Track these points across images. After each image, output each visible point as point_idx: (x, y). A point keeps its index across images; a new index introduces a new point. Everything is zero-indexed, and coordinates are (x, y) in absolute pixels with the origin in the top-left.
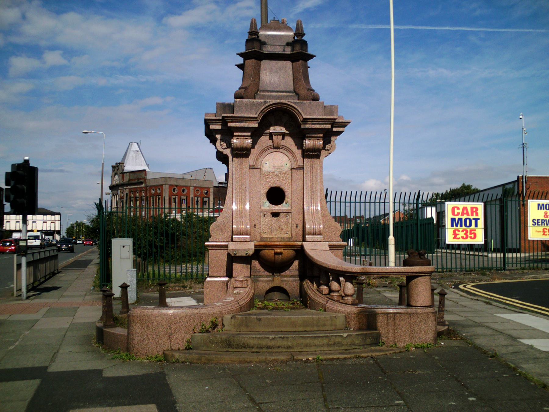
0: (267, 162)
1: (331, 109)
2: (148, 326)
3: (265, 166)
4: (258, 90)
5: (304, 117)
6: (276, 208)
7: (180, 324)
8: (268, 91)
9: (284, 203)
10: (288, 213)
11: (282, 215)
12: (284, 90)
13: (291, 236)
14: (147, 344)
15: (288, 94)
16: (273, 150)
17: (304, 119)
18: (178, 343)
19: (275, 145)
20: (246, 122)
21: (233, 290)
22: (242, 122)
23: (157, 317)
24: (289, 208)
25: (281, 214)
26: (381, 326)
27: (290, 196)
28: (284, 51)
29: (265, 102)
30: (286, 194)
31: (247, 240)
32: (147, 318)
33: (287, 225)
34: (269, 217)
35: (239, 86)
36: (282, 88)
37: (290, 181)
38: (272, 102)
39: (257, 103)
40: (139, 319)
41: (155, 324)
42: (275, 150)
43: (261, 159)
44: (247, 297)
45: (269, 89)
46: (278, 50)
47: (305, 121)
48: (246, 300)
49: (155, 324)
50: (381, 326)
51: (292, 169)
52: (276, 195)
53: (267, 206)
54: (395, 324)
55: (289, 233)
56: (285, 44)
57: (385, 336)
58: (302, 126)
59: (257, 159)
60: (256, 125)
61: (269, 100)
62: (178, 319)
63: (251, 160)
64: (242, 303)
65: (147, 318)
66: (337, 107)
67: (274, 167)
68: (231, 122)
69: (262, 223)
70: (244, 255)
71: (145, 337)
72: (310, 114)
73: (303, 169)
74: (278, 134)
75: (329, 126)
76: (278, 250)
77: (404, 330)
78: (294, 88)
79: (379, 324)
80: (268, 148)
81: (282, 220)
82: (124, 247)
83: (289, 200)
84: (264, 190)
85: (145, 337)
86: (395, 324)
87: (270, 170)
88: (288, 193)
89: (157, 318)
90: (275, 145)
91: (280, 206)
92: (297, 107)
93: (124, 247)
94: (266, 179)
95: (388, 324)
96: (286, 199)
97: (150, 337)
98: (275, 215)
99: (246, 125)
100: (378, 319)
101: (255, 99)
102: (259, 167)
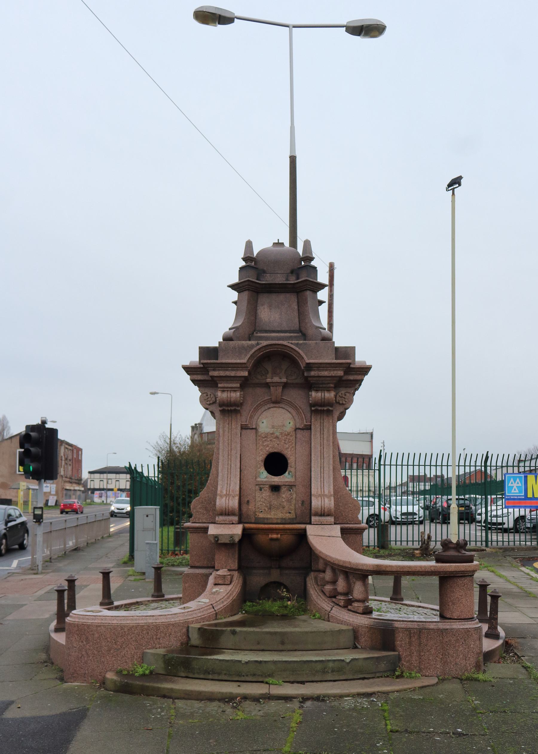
0: (264, 421)
1: (349, 352)
2: (87, 638)
3: (261, 425)
4: (255, 330)
5: (308, 361)
6: (276, 480)
7: (129, 637)
8: (266, 331)
9: (287, 472)
10: (291, 486)
11: (283, 489)
12: (287, 329)
13: (294, 517)
14: (86, 662)
15: (292, 334)
16: (272, 405)
17: (308, 364)
18: (126, 662)
19: (273, 400)
20: (232, 370)
21: (212, 589)
22: (227, 370)
23: (100, 626)
24: (293, 480)
25: (283, 487)
26: (401, 646)
27: (293, 464)
28: (287, 280)
29: (258, 344)
30: (289, 461)
31: (234, 522)
32: (86, 628)
33: (289, 501)
34: (266, 493)
35: (230, 327)
36: (285, 327)
37: (294, 444)
38: (264, 343)
39: (248, 346)
40: (76, 629)
41: (96, 635)
42: (274, 405)
43: (256, 417)
44: (228, 598)
45: (267, 329)
46: (280, 279)
47: (309, 367)
48: (225, 603)
49: (96, 635)
50: (401, 646)
51: (296, 429)
52: (276, 463)
53: (264, 476)
54: (420, 644)
55: (293, 512)
56: (289, 271)
57: (407, 659)
58: (306, 374)
59: (251, 417)
60: (246, 374)
61: (261, 342)
62: (126, 630)
63: (244, 418)
64: (219, 607)
65: (86, 628)
66: (353, 348)
67: (273, 427)
68: (214, 370)
69: (258, 499)
70: (229, 542)
71: (84, 653)
72: (316, 358)
73: (310, 429)
74: (276, 384)
75: (340, 373)
76: (275, 536)
77: (433, 651)
78: (300, 327)
79: (398, 643)
80: (266, 402)
81: (284, 496)
82: (147, 516)
83: (292, 470)
84: (261, 457)
85: (84, 653)
86: (420, 644)
87: (269, 430)
88: (291, 461)
89: (99, 628)
90: (273, 400)
91: (282, 476)
92: (297, 349)
93: (147, 516)
94: (263, 442)
95: (410, 643)
96: (289, 468)
97: (90, 652)
98: (275, 488)
99: (233, 374)
100: (397, 635)
101: (250, 340)
102: (254, 427)
